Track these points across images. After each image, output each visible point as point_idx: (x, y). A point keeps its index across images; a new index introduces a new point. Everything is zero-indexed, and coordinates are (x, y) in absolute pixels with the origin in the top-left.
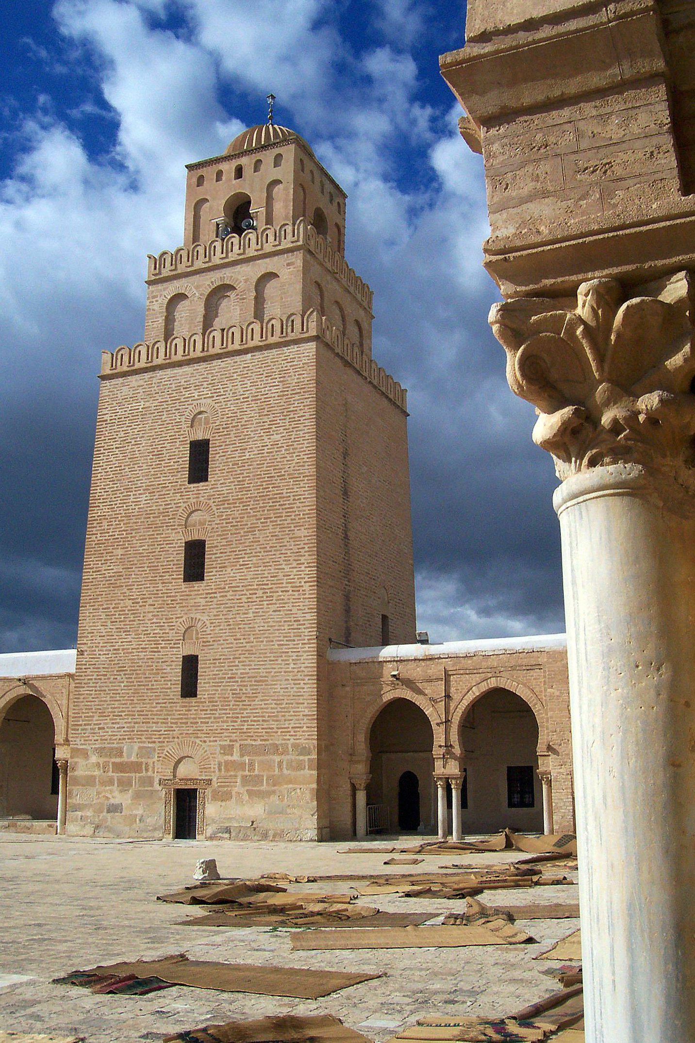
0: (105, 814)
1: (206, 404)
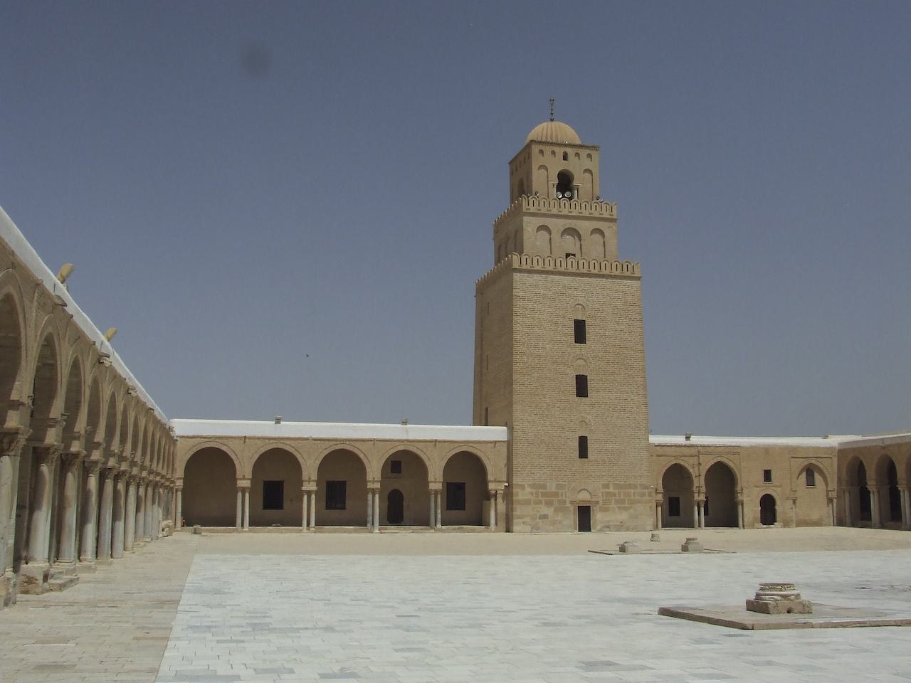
0: (537, 520)
1: (582, 300)
